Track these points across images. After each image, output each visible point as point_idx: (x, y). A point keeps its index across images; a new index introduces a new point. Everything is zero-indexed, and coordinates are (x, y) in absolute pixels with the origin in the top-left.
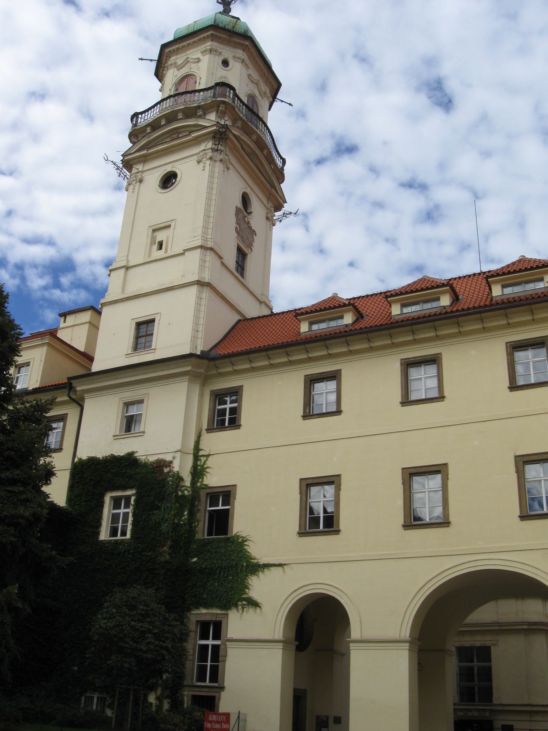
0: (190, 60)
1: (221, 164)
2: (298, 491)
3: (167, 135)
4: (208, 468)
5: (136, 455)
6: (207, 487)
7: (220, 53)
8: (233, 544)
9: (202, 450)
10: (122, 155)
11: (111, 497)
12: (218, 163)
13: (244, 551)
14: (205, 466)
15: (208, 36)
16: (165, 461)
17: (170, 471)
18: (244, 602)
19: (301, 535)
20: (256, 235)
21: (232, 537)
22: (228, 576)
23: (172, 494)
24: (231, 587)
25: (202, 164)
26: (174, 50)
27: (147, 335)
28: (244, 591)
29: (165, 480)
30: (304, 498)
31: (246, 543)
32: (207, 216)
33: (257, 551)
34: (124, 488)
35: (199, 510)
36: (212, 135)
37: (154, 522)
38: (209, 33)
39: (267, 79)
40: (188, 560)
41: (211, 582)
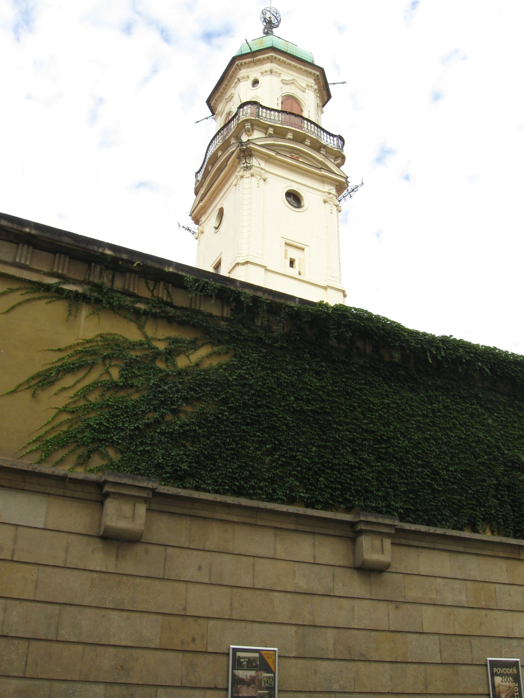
0: (295, 82)
3: (289, 150)
15: (314, 74)
26: (279, 60)
36: (338, 184)
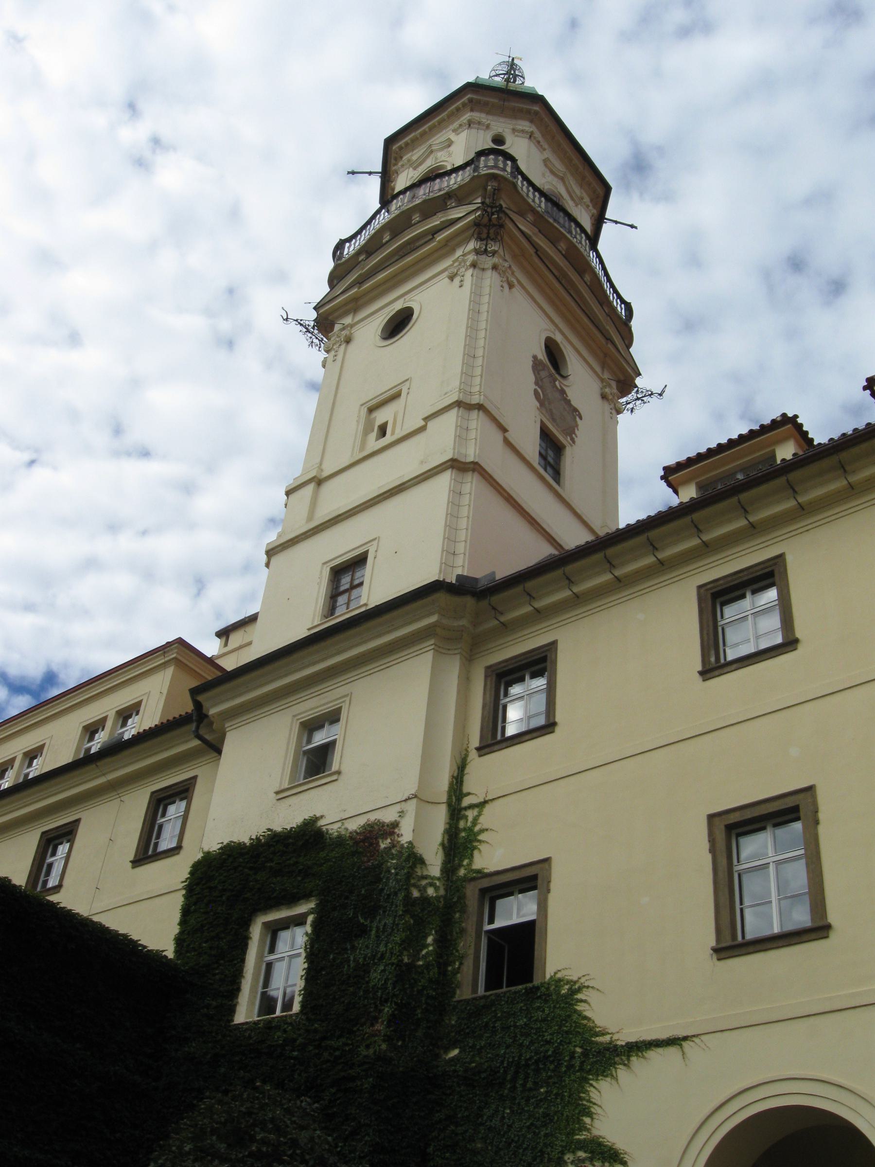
1: (495, 274)
2: (706, 845)
4: (482, 831)
5: (321, 823)
6: (481, 874)
7: (488, 127)
8: (546, 1001)
9: (469, 794)
10: (315, 308)
11: (264, 924)
12: (489, 273)
13: (575, 1017)
14: (477, 829)
15: (464, 105)
16: (380, 824)
17: (393, 845)
18: (581, 1154)
19: (723, 955)
20: (581, 418)
21: (542, 984)
22: (537, 1086)
23: (396, 894)
24: (546, 1115)
25: (457, 280)
26: (407, 144)
27: (353, 587)
28: (579, 1121)
29: (380, 866)
30: (723, 862)
31: (579, 996)
32: (469, 356)
33: (610, 1013)
34: (292, 900)
35: (463, 931)
37: (352, 964)
38: (465, 99)
39: (583, 178)
40: (437, 1056)
41: (494, 1106)
